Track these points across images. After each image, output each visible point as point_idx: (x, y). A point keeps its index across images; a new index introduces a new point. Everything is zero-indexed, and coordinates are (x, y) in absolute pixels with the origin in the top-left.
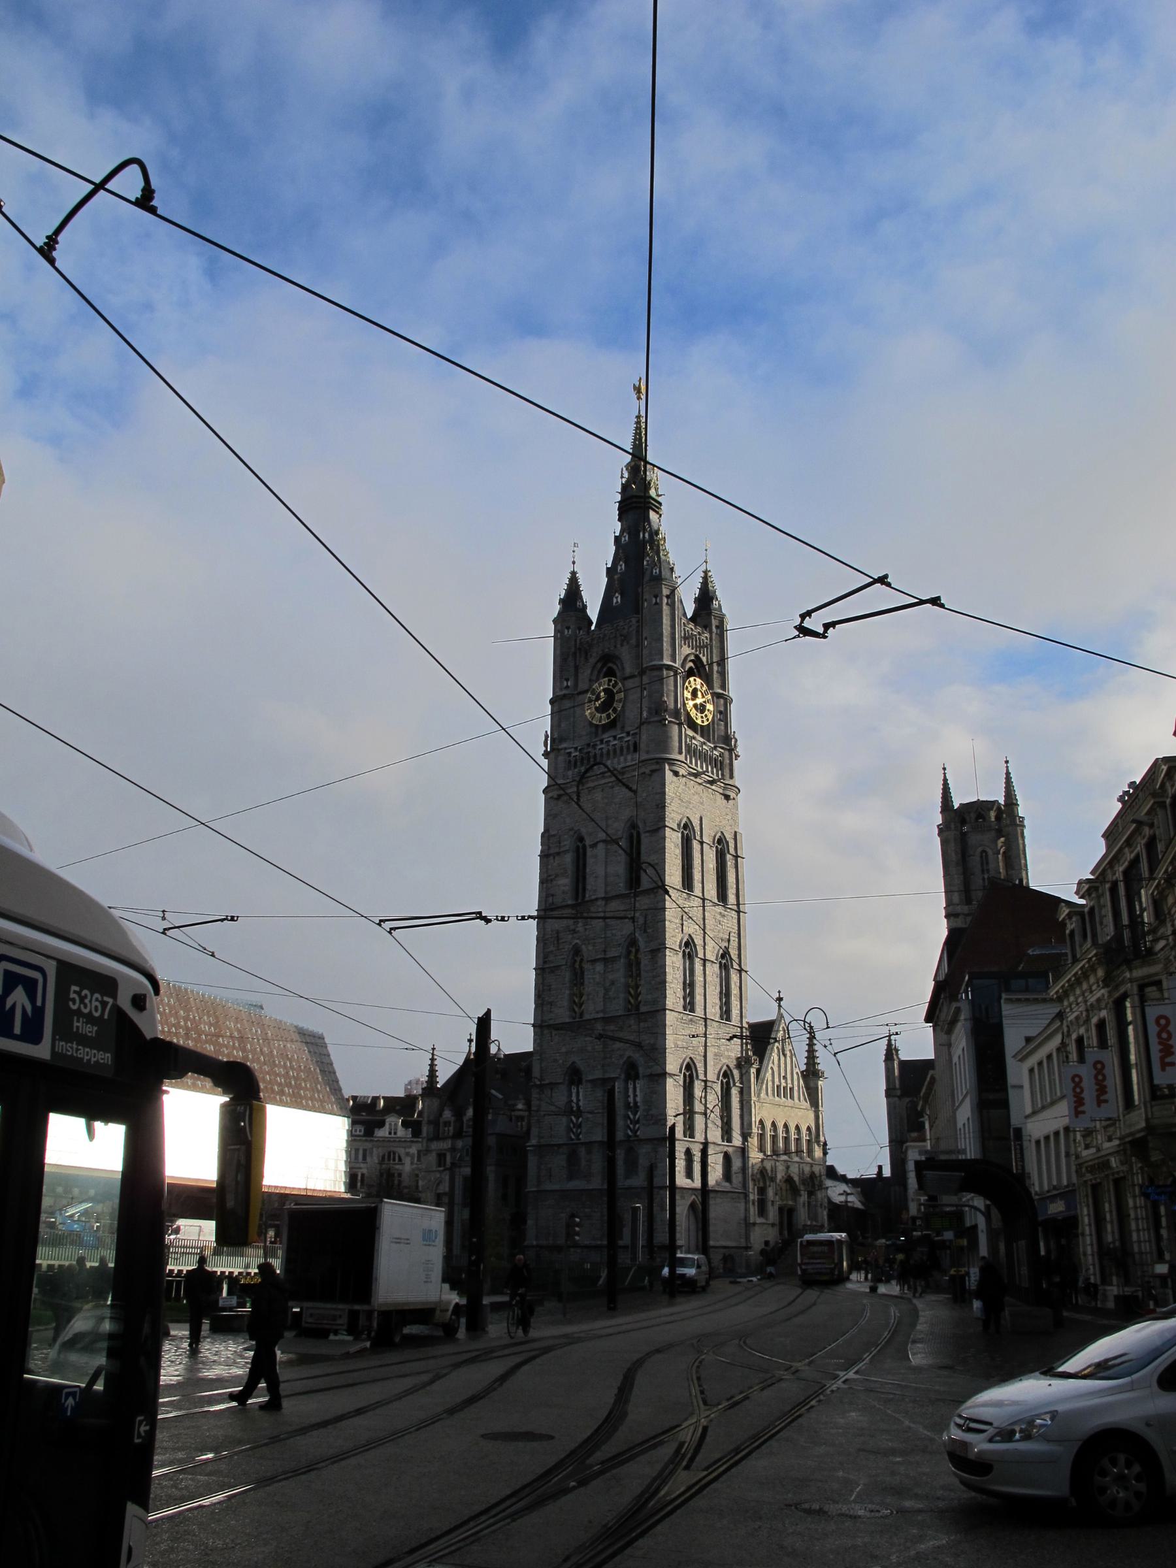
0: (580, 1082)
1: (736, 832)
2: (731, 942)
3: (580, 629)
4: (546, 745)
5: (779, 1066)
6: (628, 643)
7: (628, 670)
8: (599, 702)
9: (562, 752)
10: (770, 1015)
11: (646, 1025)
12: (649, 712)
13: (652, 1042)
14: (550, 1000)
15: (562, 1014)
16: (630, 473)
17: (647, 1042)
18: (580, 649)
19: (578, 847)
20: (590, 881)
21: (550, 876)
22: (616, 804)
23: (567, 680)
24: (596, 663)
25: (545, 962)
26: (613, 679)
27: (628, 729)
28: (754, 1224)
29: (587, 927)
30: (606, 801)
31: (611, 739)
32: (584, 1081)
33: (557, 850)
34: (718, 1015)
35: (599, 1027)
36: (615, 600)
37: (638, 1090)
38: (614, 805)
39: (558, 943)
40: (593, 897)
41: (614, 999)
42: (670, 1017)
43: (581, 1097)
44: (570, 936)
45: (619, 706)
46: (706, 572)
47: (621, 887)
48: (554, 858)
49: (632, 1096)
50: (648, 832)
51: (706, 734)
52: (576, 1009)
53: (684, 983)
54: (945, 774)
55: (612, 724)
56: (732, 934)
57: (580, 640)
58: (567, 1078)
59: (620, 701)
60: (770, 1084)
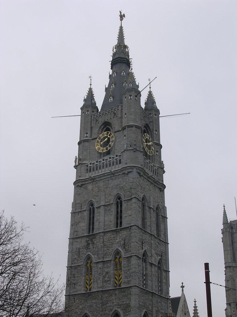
3: (93, 112)
4: (76, 163)
8: (103, 142)
9: (84, 165)
11: (124, 294)
14: (74, 282)
15: (81, 290)
17: (125, 302)
19: (90, 208)
20: (96, 224)
21: (76, 222)
22: (110, 188)
23: (87, 133)
24: (101, 126)
25: (72, 264)
26: (109, 132)
29: (94, 246)
31: (108, 158)
36: (110, 100)
39: (79, 254)
40: (98, 232)
41: (108, 281)
44: (85, 251)
46: (150, 92)
48: (78, 214)
52: (88, 287)
54: (224, 208)
55: (108, 153)
56: (163, 253)
59: (112, 142)
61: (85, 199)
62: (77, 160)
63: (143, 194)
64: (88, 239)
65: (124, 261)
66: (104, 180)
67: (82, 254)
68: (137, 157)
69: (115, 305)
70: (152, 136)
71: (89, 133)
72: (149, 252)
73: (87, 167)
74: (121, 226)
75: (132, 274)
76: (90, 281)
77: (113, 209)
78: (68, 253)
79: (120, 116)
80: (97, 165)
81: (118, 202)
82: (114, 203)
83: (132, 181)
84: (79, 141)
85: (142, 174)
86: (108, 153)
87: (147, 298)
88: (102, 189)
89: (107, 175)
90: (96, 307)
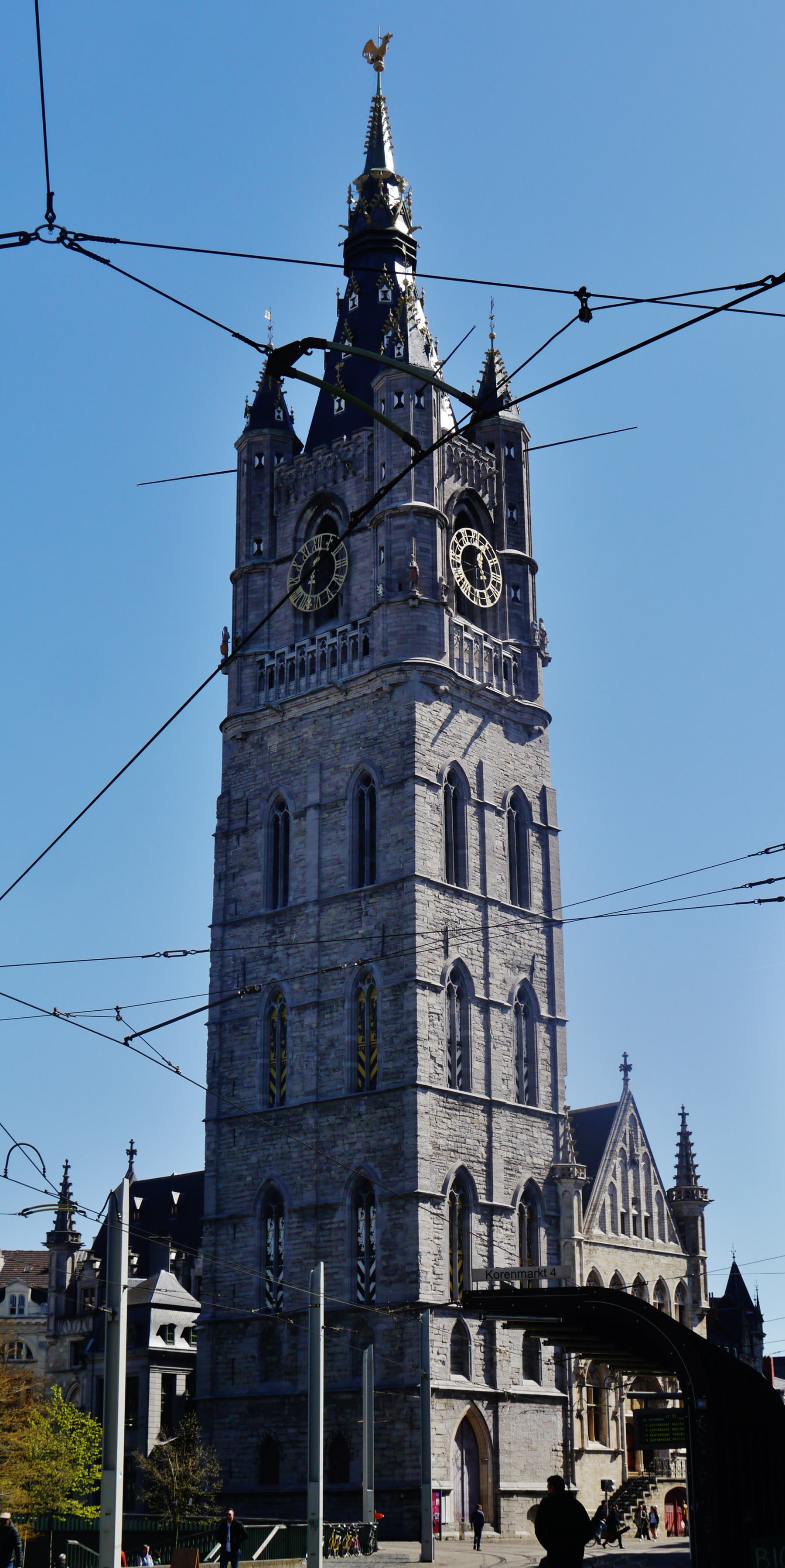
0: (280, 1213)
1: (544, 787)
2: (537, 970)
5: (625, 1182)
6: (355, 474)
9: (250, 660)
10: (609, 1095)
11: (386, 1114)
12: (387, 588)
13: (396, 1141)
14: (233, 1076)
16: (362, 194)
17: (387, 1141)
18: (278, 488)
19: (276, 818)
20: (295, 873)
22: (336, 744)
23: (259, 542)
24: (304, 512)
26: (331, 535)
27: (353, 618)
28: (581, 1452)
29: (291, 951)
30: (320, 738)
31: (328, 635)
32: (286, 1211)
33: (242, 824)
34: (513, 1095)
35: (310, 1120)
38: (332, 746)
39: (244, 980)
40: (301, 901)
41: (334, 1070)
42: (424, 1100)
44: (263, 968)
45: (339, 579)
47: (343, 882)
48: (238, 838)
49: (363, 1235)
50: (387, 787)
51: (490, 624)
52: (275, 1090)
53: (450, 1042)
57: (279, 473)
58: (259, 1206)
60: (608, 1211)
61: (259, 787)
62: (230, 640)
63: (452, 759)
64: (269, 928)
65: (384, 999)
66: (313, 715)
67: (253, 979)
68: (424, 628)
69: (359, 1151)
70: (493, 534)
71: (265, 538)
72: (474, 962)
73: (262, 667)
74: (372, 881)
75: (406, 1047)
76: (282, 1071)
78: (211, 976)
80: (295, 662)
81: (362, 793)
82: (350, 796)
83: (405, 718)
84: (232, 568)
87: (469, 1120)
88: (311, 747)
90: (300, 1160)
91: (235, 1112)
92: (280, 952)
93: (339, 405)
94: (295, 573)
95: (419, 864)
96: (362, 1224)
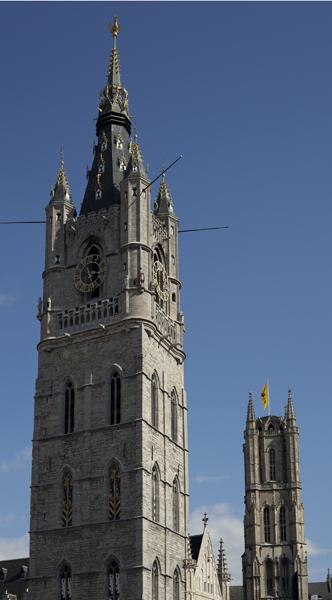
7: (110, 250)
23: (58, 257)
33: (49, 393)
35: (86, 533)
37: (118, 581)
40: (81, 430)
42: (145, 523)
43: (69, 588)
58: (59, 572)
59: (103, 274)
71: (62, 255)
74: (118, 422)
77: (106, 391)
79: (116, 226)
81: (113, 380)
82: (107, 381)
85: (152, 333)
86: (96, 293)
89: (96, 334)
91: (45, 529)
92: (69, 453)
93: (99, 194)
94: (78, 273)
95: (143, 414)
96: (111, 581)
